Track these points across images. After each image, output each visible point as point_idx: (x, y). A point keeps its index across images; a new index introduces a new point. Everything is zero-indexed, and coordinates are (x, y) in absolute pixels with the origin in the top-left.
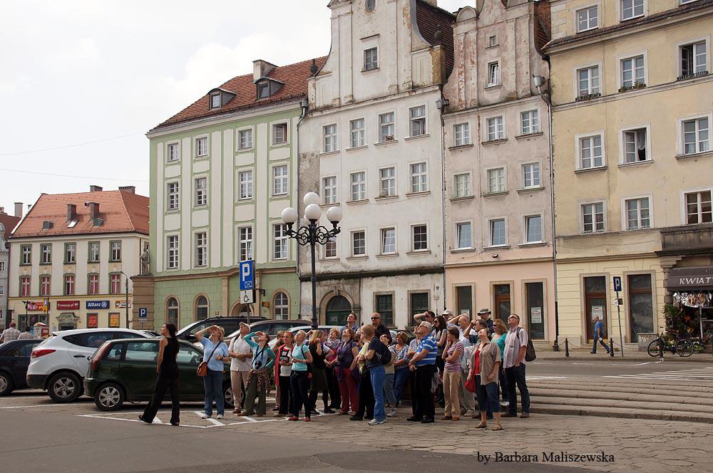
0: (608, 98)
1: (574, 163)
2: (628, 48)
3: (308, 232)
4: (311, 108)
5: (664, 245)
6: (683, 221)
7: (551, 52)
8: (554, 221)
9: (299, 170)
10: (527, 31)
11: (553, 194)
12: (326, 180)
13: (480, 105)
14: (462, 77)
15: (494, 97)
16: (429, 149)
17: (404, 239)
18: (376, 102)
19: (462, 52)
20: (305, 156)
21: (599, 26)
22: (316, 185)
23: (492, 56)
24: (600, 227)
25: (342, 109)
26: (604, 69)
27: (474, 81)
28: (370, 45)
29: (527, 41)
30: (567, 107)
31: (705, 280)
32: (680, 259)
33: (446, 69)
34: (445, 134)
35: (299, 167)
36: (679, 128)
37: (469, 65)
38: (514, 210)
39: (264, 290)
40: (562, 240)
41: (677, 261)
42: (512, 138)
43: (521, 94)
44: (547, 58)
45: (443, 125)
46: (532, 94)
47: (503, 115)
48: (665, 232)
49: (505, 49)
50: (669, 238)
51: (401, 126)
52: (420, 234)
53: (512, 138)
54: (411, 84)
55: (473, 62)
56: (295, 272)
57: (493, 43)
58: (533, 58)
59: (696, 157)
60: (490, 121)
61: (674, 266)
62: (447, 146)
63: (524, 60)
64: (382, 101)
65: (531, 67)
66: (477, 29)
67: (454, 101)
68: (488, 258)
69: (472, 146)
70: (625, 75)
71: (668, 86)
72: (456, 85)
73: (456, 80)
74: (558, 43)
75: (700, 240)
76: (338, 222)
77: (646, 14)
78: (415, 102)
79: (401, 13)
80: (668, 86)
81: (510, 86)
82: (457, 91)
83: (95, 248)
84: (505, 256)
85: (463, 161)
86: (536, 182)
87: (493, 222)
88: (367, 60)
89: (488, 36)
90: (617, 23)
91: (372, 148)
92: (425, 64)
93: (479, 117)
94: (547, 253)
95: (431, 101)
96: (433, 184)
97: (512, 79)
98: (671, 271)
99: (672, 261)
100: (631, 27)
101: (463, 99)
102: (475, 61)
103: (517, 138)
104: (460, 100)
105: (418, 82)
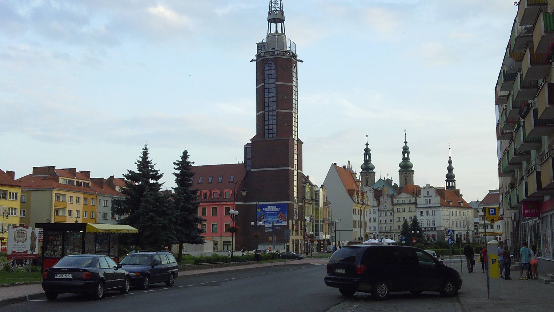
10: (390, 202)
15: (386, 210)
16: (376, 216)
23: (386, 204)
24: (400, 229)
33: (379, 204)
38: (389, 226)
44: (393, 206)
46: (391, 210)
51: (372, 211)
52: (375, 227)
67: (380, 209)
71: (407, 212)
74: (395, 204)
80: (407, 212)
81: (388, 209)
85: (381, 218)
92: (375, 203)
95: (377, 209)
96: (377, 220)
100: (403, 204)
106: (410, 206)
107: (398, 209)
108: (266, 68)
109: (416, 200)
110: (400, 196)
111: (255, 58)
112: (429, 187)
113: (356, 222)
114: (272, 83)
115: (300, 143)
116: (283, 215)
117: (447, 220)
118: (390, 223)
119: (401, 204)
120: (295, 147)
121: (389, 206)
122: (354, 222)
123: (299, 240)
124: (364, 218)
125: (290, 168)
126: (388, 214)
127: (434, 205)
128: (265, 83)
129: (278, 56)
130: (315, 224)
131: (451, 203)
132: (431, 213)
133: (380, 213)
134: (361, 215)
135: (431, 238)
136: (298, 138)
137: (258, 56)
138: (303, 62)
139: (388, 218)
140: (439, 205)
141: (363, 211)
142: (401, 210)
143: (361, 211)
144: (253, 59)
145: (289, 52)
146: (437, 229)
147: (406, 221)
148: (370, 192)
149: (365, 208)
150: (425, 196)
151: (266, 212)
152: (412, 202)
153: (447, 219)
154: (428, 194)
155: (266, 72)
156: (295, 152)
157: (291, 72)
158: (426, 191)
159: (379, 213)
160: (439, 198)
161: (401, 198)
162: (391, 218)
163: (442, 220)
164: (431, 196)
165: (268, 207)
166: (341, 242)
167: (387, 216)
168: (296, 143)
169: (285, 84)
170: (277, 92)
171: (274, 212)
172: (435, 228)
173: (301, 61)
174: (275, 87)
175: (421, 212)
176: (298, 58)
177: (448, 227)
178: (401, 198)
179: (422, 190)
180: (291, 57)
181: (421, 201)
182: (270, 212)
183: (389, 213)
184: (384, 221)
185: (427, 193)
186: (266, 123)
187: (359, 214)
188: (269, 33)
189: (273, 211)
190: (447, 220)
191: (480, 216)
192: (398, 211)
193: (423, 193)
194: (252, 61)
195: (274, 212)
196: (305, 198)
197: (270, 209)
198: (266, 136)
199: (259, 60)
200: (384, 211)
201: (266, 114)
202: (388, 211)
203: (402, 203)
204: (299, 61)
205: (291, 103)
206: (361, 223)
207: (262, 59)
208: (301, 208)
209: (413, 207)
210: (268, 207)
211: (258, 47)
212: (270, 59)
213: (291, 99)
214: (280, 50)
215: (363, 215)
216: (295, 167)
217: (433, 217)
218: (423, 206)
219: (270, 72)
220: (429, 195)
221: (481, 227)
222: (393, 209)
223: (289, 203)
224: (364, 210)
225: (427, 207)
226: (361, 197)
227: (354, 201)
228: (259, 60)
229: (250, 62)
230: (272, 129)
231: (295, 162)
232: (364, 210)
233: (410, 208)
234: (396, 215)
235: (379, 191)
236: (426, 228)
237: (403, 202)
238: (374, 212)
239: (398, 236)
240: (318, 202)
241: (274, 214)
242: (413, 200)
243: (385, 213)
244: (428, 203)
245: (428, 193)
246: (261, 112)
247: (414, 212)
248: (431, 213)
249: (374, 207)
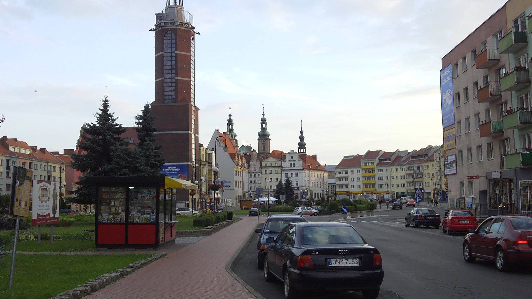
2: (270, 169)
10: (259, 165)
33: (249, 167)
44: (261, 168)
48: (274, 189)
67: (250, 171)
73: (250, 169)
74: (263, 167)
81: (257, 171)
85: (251, 179)
106: (276, 169)
107: (265, 171)
108: (165, 38)
109: (282, 164)
110: (267, 160)
111: (154, 28)
112: (293, 152)
113: (237, 182)
114: (171, 52)
115: (197, 109)
116: (183, 175)
117: (308, 181)
118: (258, 184)
119: (268, 167)
120: (193, 113)
121: (258, 169)
122: (235, 182)
123: (197, 199)
124: (243, 178)
125: (190, 132)
126: (257, 175)
128: (165, 52)
129: (178, 27)
130: (208, 183)
131: (311, 166)
132: (294, 175)
133: (250, 175)
134: (240, 176)
136: (195, 105)
137: (157, 26)
138: (200, 34)
139: (257, 179)
140: (302, 168)
141: (241, 172)
142: (268, 172)
143: (240, 172)
144: (152, 29)
145: (188, 24)
147: (280, 182)
149: (243, 170)
151: (166, 172)
152: (278, 165)
153: (308, 180)
154: (292, 159)
155: (166, 42)
156: (193, 117)
157: (190, 42)
158: (290, 156)
159: (249, 174)
160: (302, 162)
161: (268, 161)
162: (260, 179)
163: (304, 181)
164: (295, 160)
165: (168, 168)
166: (226, 200)
167: (256, 177)
168: (193, 108)
169: (184, 53)
170: (176, 61)
171: (174, 173)
172: (298, 188)
173: (198, 33)
174: (175, 56)
175: (286, 174)
176: (195, 30)
177: (308, 187)
178: (268, 161)
179: (287, 156)
180: (190, 28)
181: (286, 165)
182: (169, 172)
183: (258, 175)
184: (253, 182)
185: (292, 158)
186: (166, 89)
187: (239, 175)
188: (168, 5)
189: (172, 172)
190: (308, 181)
191: (337, 178)
192: (266, 173)
193: (288, 158)
194: (151, 30)
195: (174, 173)
196: (200, 160)
197: (171, 170)
198: (166, 101)
199: (157, 30)
201: (166, 80)
202: (257, 172)
203: (269, 166)
204: (196, 33)
205: (190, 72)
206: (240, 182)
207: (162, 29)
208: (198, 169)
209: (279, 170)
210: (168, 168)
211: (157, 17)
212: (169, 30)
213: (190, 68)
214: (180, 21)
215: (241, 176)
216: (193, 131)
217: (297, 178)
219: (170, 41)
220: (293, 160)
221: (337, 187)
222: (261, 171)
223: (188, 164)
224: (242, 172)
225: (291, 170)
226: (240, 160)
227: (235, 163)
228: (157, 30)
229: (149, 31)
230: (172, 95)
231: (193, 127)
232: (242, 172)
233: (276, 170)
234: (264, 176)
235: (248, 155)
237: (270, 165)
239: (265, 195)
240: (211, 164)
241: (176, 174)
242: (279, 163)
243: (254, 175)
244: (292, 166)
245: (292, 157)
246: (161, 79)
247: (280, 174)
248: (294, 175)
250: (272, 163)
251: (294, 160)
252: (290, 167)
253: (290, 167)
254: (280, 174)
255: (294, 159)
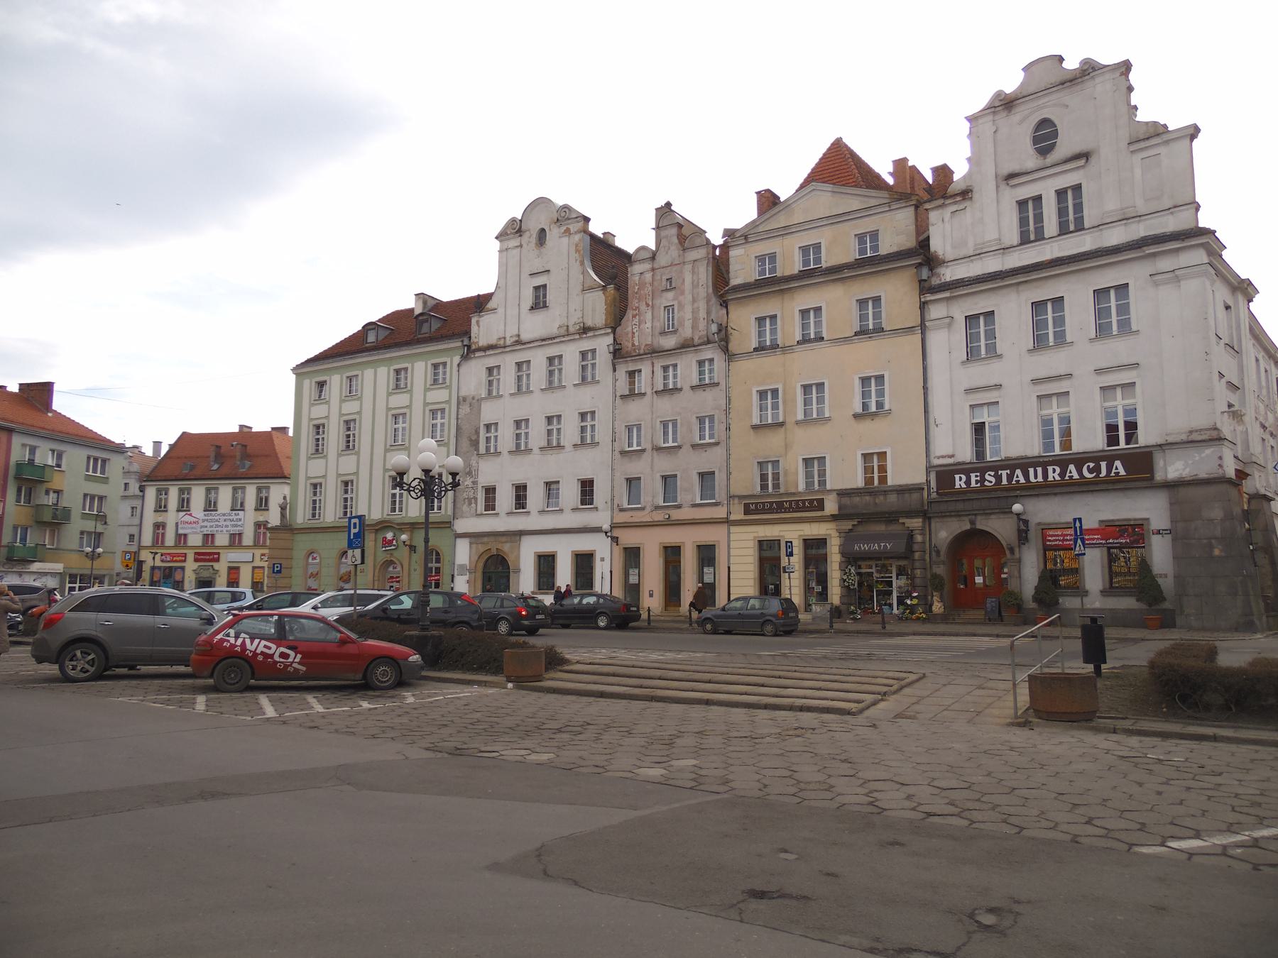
0: (786, 349)
1: (751, 416)
3: (422, 485)
4: (473, 347)
5: (840, 508)
6: (859, 482)
7: (730, 298)
8: (728, 479)
9: (458, 415)
11: (728, 450)
12: (488, 427)
13: (654, 352)
14: (636, 320)
15: (669, 342)
16: (599, 397)
17: (570, 493)
18: (544, 343)
19: (636, 293)
20: (465, 399)
21: (779, 274)
22: (476, 431)
24: (776, 486)
25: (508, 349)
26: (783, 318)
27: (649, 325)
28: (539, 281)
29: (705, 286)
30: (745, 357)
31: (880, 546)
32: (856, 523)
33: (618, 312)
34: (616, 380)
35: (458, 411)
36: (857, 384)
37: (643, 307)
38: (688, 466)
39: (415, 547)
40: (736, 501)
41: (853, 525)
42: (686, 388)
43: (696, 341)
44: (725, 304)
45: (615, 370)
46: (709, 342)
47: (679, 362)
48: (842, 493)
49: (682, 293)
50: (846, 500)
53: (686, 388)
54: (582, 325)
55: (648, 305)
56: (450, 527)
57: (670, 286)
58: (711, 303)
59: (874, 415)
60: (665, 368)
61: (850, 530)
62: (618, 394)
63: (702, 305)
64: (550, 342)
65: (708, 313)
66: (653, 269)
67: (627, 345)
68: (659, 516)
69: (644, 394)
70: (805, 326)
71: (846, 340)
72: (629, 329)
73: (629, 324)
75: (876, 504)
76: (458, 474)
77: (824, 265)
78: (586, 345)
79: (573, 249)
80: (846, 340)
81: (687, 332)
82: (630, 335)
83: (213, 495)
84: (676, 515)
85: (636, 410)
86: (711, 436)
87: (630, 481)
88: (537, 297)
89: (664, 278)
90: (796, 272)
91: (537, 394)
92: (596, 307)
93: (653, 363)
94: (720, 513)
95: (603, 344)
96: (603, 433)
97: (688, 324)
98: (847, 537)
99: (847, 525)
100: (812, 275)
101: (637, 344)
102: (650, 303)
103: (693, 388)
104: (633, 345)
105: (589, 323)
106: (867, 289)
109: (922, 228)
118: (694, 446)
121: (695, 312)
127: (1115, 237)
135: (1093, 567)
139: (687, 406)
142: (791, 329)
146: (1173, 468)
148: (568, 231)
150: (1015, 167)
152: (884, 249)
159: (622, 370)
185: (1036, 140)
200: (654, 352)
202: (686, 346)
203: (797, 267)
218: (993, 265)
236: (1024, 464)
237: (806, 262)
238: (586, 379)
243: (659, 373)
244: (1051, 226)
245: (1045, 136)
247: (909, 330)
249: (585, 330)
250: (823, 237)
251: (1077, 149)
252: (1015, 240)
253: (1025, 240)
254: (909, 330)
255: (1065, 147)
